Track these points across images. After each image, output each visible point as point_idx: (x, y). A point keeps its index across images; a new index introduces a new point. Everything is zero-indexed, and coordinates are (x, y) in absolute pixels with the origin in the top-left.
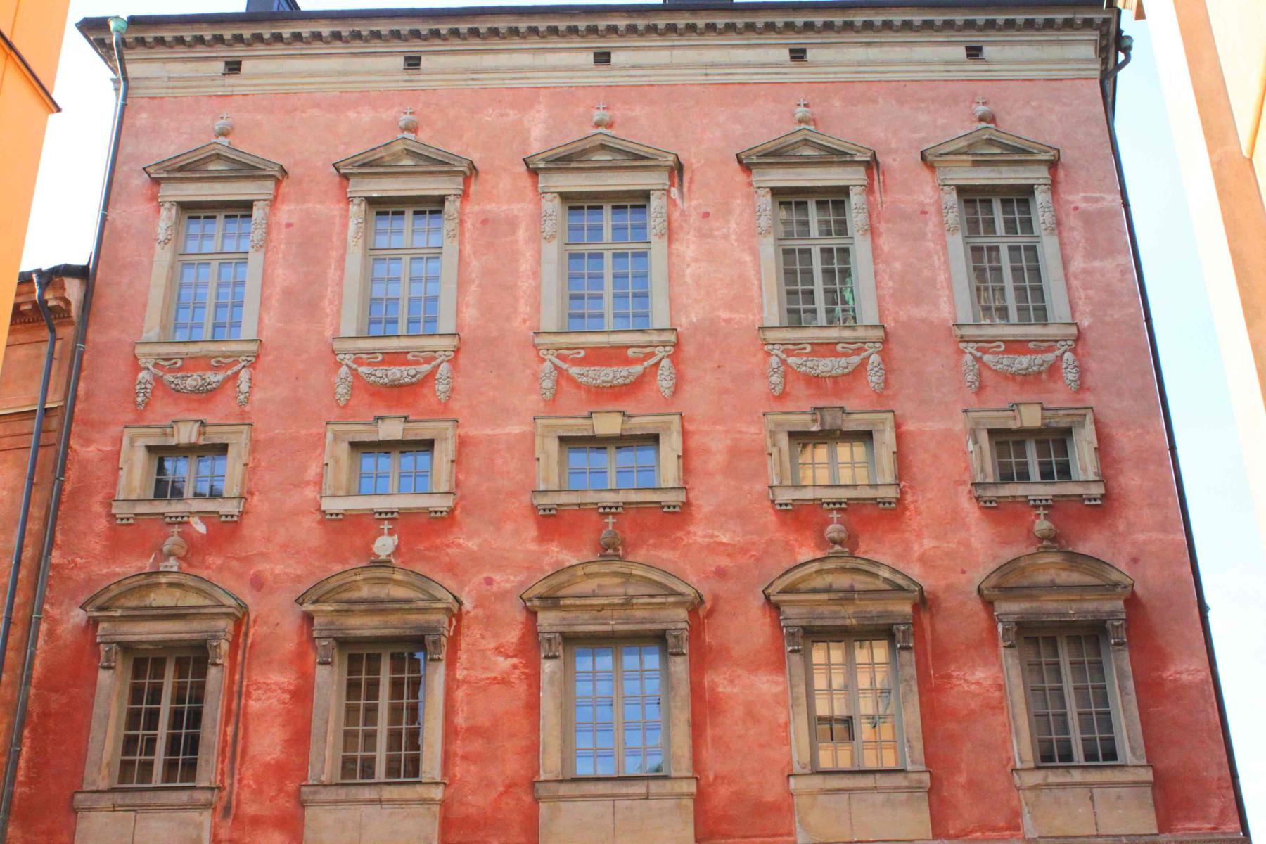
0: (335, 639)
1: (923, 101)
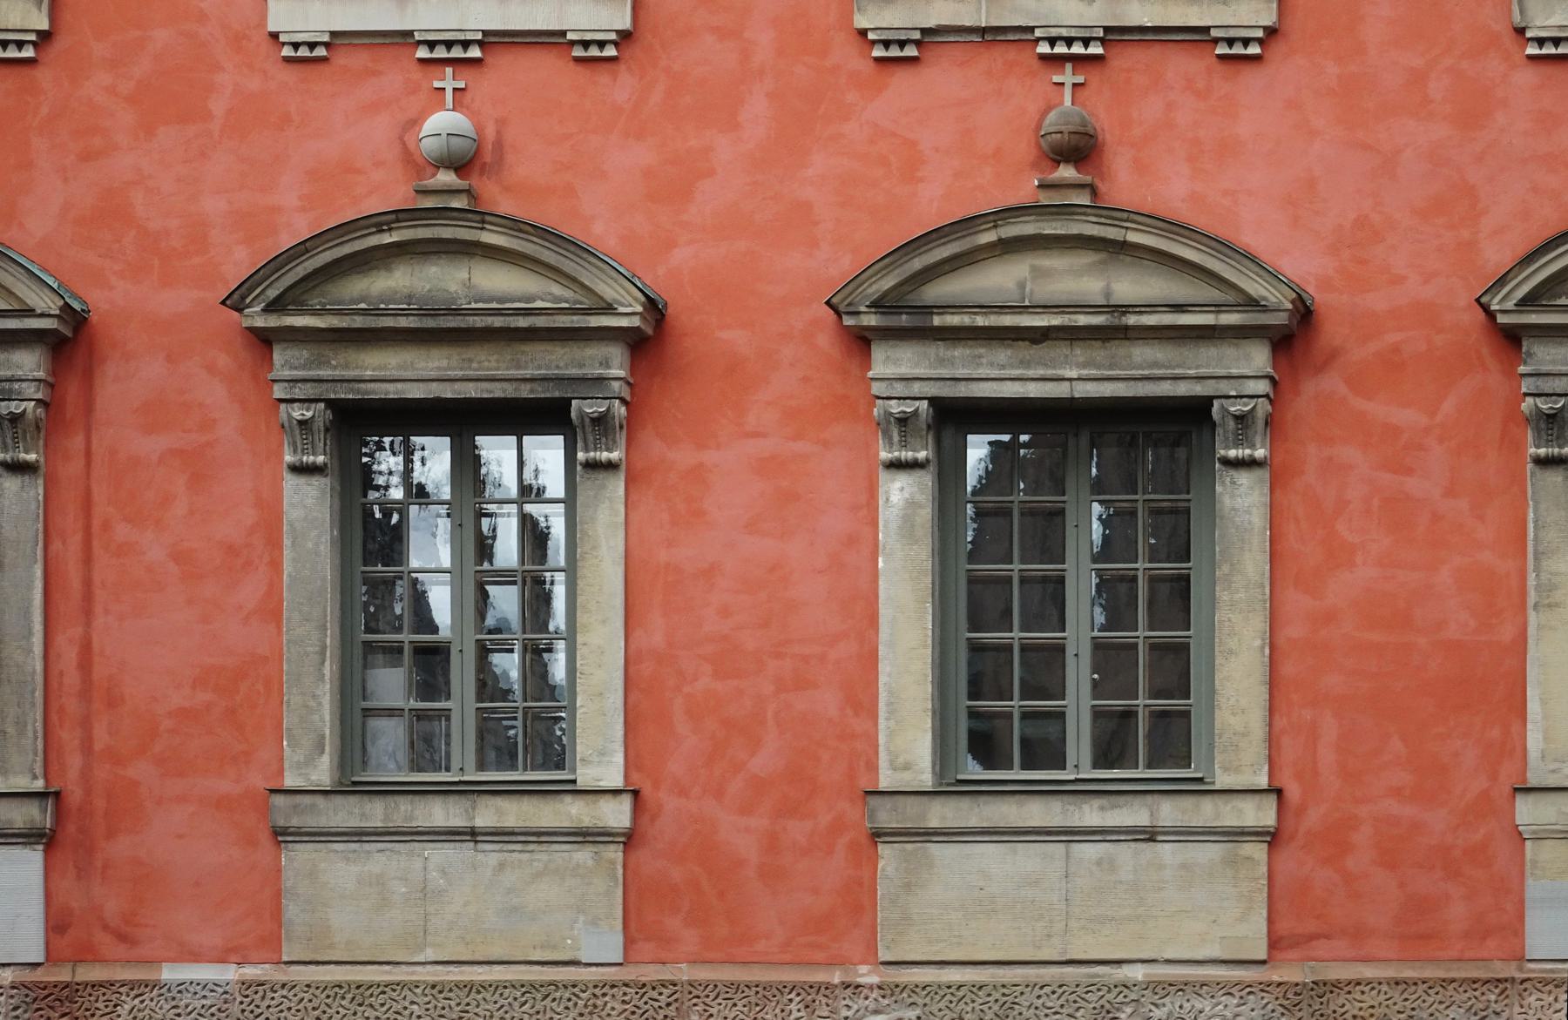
0: (330, 403)
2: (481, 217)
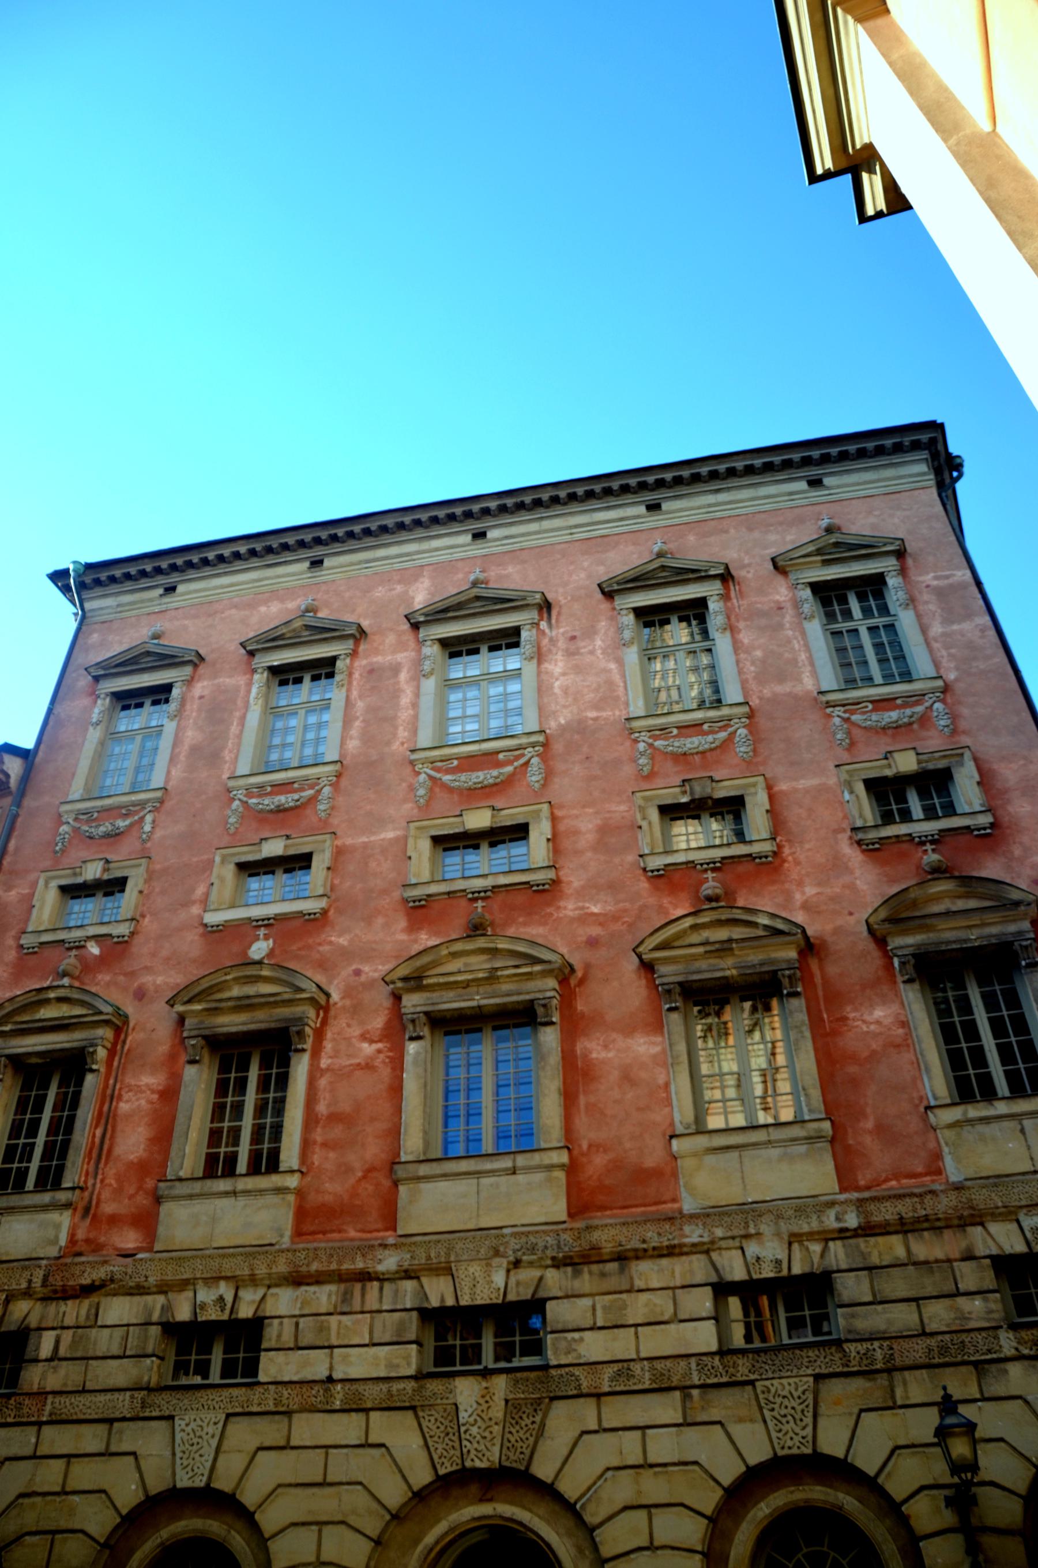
0: (205, 1037)
1: (772, 525)
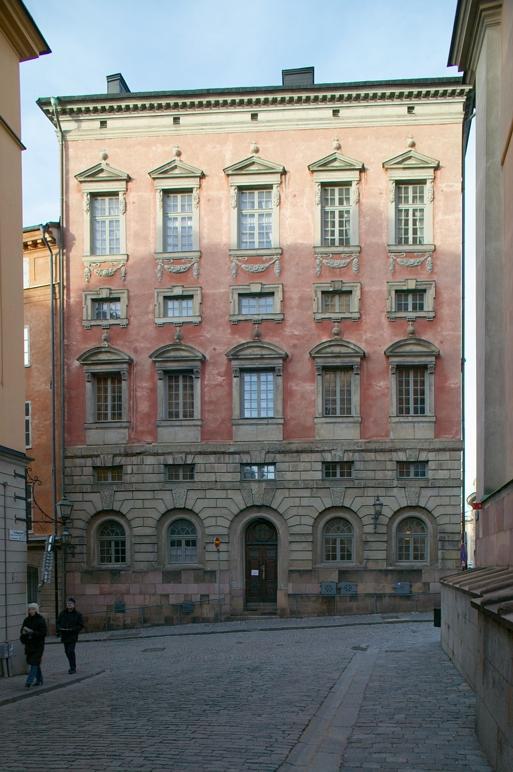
2: (181, 345)
